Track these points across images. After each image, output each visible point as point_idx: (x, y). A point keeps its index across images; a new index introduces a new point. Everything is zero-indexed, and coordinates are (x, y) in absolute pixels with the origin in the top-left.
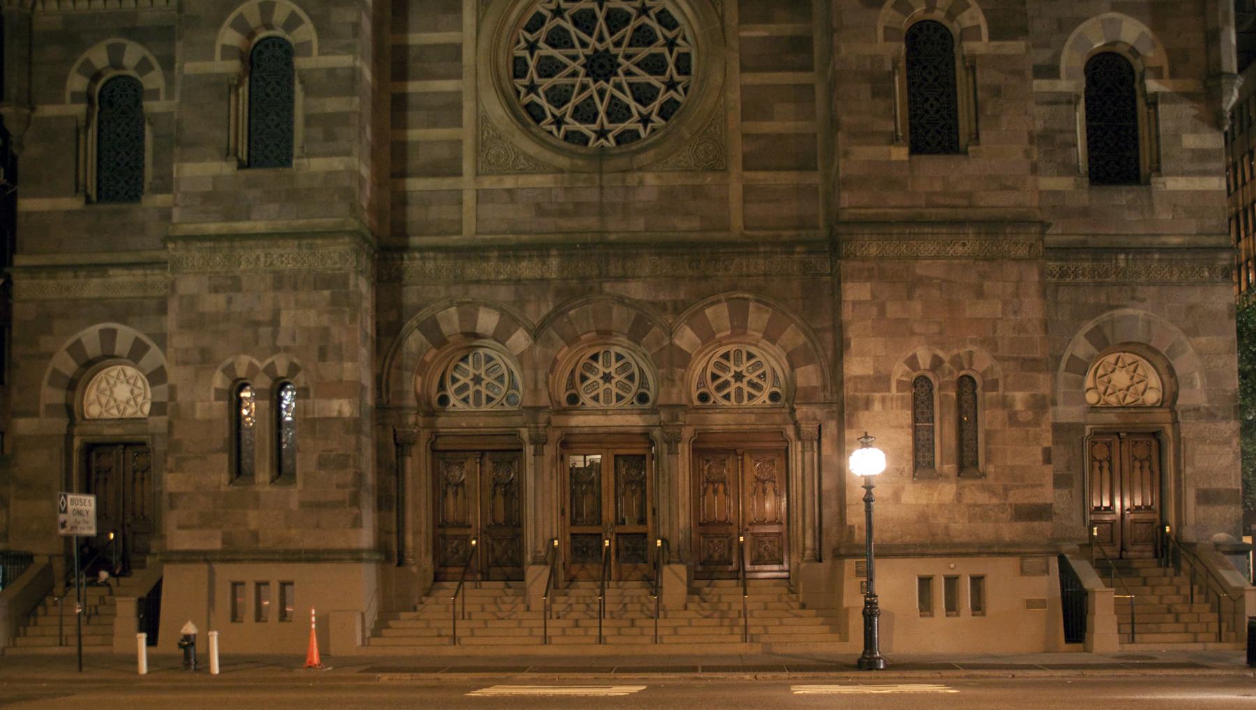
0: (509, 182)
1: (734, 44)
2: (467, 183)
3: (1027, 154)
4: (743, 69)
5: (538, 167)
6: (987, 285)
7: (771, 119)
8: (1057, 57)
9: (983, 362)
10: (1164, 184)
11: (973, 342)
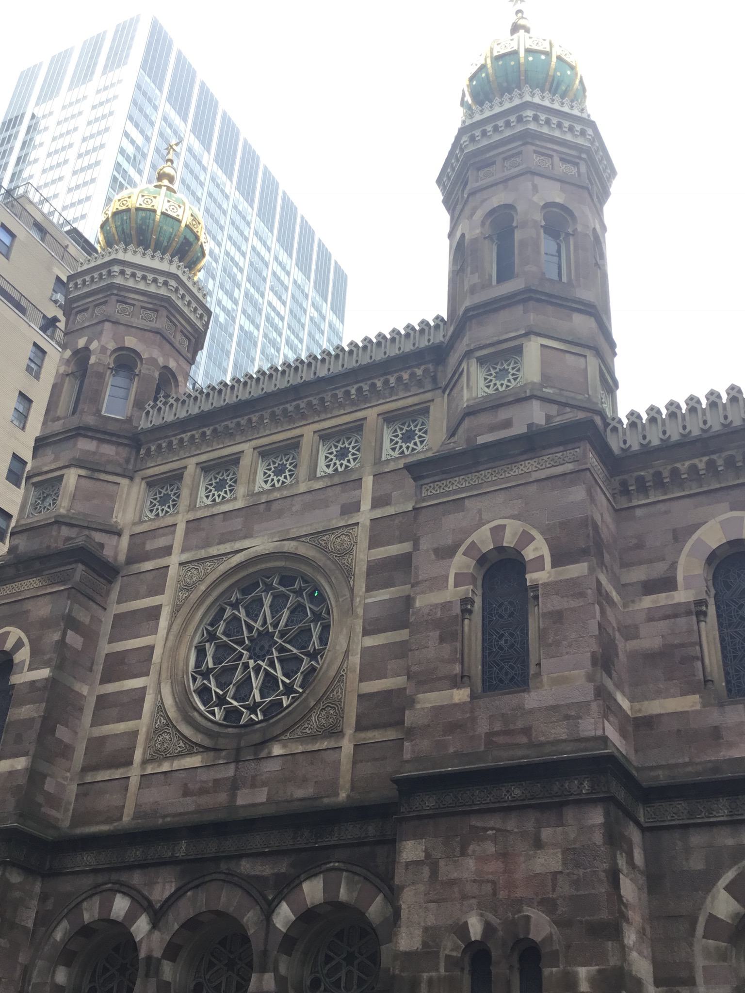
0: (166, 767)
1: (360, 611)
2: (134, 773)
3: (590, 678)
4: (366, 633)
5: (192, 748)
6: (546, 834)
8: (673, 566)
9: (541, 926)
11: (530, 903)
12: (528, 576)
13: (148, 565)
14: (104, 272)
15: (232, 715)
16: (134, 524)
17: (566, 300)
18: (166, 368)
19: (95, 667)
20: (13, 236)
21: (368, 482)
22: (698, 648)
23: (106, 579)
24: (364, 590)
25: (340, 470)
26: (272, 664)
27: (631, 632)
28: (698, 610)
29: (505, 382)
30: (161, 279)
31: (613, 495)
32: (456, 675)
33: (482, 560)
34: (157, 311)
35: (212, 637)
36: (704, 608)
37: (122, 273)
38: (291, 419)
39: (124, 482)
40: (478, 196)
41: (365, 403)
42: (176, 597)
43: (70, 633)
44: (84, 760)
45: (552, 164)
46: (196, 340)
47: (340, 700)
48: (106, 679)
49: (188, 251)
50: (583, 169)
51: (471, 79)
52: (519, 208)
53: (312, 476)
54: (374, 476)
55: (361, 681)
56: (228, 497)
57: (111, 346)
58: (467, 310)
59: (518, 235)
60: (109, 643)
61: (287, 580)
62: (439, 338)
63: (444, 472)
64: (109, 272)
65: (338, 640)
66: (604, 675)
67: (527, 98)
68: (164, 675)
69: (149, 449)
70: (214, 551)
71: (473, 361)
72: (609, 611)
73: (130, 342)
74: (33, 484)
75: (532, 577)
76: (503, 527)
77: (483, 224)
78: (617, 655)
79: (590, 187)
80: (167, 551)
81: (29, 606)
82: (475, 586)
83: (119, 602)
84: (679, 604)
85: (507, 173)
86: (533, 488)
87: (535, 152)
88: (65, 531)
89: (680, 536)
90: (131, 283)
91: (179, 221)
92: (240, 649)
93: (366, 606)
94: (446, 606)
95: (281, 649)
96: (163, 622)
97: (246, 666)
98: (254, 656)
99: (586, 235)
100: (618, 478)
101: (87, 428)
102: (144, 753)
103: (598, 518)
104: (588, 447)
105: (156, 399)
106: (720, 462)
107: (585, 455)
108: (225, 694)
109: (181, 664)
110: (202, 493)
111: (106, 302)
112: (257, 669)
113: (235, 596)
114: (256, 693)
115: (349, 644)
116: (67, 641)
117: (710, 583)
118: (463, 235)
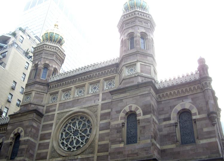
3: (151, 141)
4: (100, 130)
7: (104, 141)
8: (170, 115)
10: (200, 142)
12: (137, 118)
13: (50, 114)
14: (42, 47)
15: (69, 149)
16: (47, 104)
17: (146, 54)
18: (55, 68)
19: (38, 137)
20: (23, 38)
21: (101, 95)
22: (175, 133)
23: (41, 117)
24: (100, 120)
25: (94, 92)
26: (78, 137)
27: (160, 130)
28: (175, 125)
29: (132, 72)
30: (54, 48)
31: (157, 98)
32: (121, 141)
33: (127, 114)
34: (53, 55)
35: (65, 131)
36: (177, 124)
37: (46, 47)
38: (84, 80)
39: (46, 94)
40: (126, 30)
41: (100, 76)
42: (57, 121)
43: (33, 129)
44: (36, 158)
45: (142, 23)
46: (62, 61)
47: (94, 146)
48: (41, 139)
49: (61, 42)
50: (149, 24)
51: (124, 5)
52: (135, 33)
53: (88, 93)
54: (102, 93)
55: (99, 141)
56: (68, 98)
57: (43, 63)
58: (123, 56)
59: (135, 39)
60: (41, 131)
61: (82, 118)
62: (117, 62)
63: (118, 93)
64: (43, 47)
65: (94, 132)
66: (154, 141)
67: (137, 10)
68: (53, 140)
69: (51, 87)
70: (65, 110)
71: (125, 67)
72: (156, 125)
73: (47, 62)
74: (25, 95)
75: (138, 118)
76: (132, 106)
77: (127, 36)
78: (157, 135)
79: (150, 28)
80: (55, 110)
81: (24, 122)
82: (125, 120)
83: (44, 122)
84: (171, 124)
85: (132, 25)
86: (139, 97)
87: (138, 21)
88: (33, 106)
89: (172, 108)
90: (48, 49)
91: (59, 35)
92: (71, 134)
93: (100, 124)
94: (118, 124)
95: (81, 134)
96: (54, 127)
97: (72, 138)
98: (74, 135)
99: (150, 39)
100: (158, 94)
101: (37, 82)
102: (49, 157)
103: (153, 104)
104: (151, 87)
105: (53, 75)
106: (180, 91)
107: (150, 90)
108: (68, 144)
109: (57, 137)
110: (63, 97)
111: (42, 53)
112: (75, 138)
113: (70, 121)
114: (75, 144)
115: (96, 133)
116: (32, 130)
117: (178, 118)
118: (123, 39)
